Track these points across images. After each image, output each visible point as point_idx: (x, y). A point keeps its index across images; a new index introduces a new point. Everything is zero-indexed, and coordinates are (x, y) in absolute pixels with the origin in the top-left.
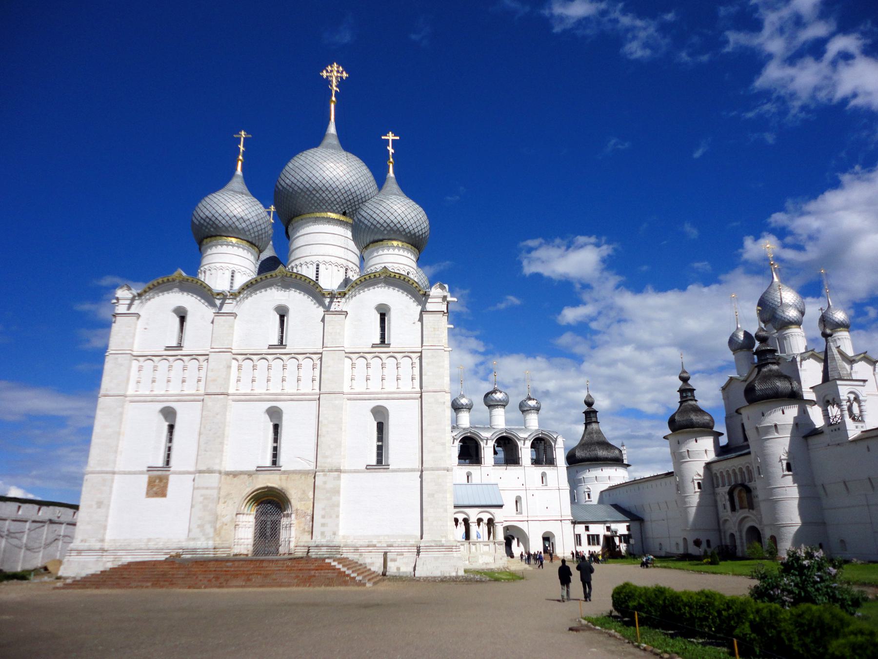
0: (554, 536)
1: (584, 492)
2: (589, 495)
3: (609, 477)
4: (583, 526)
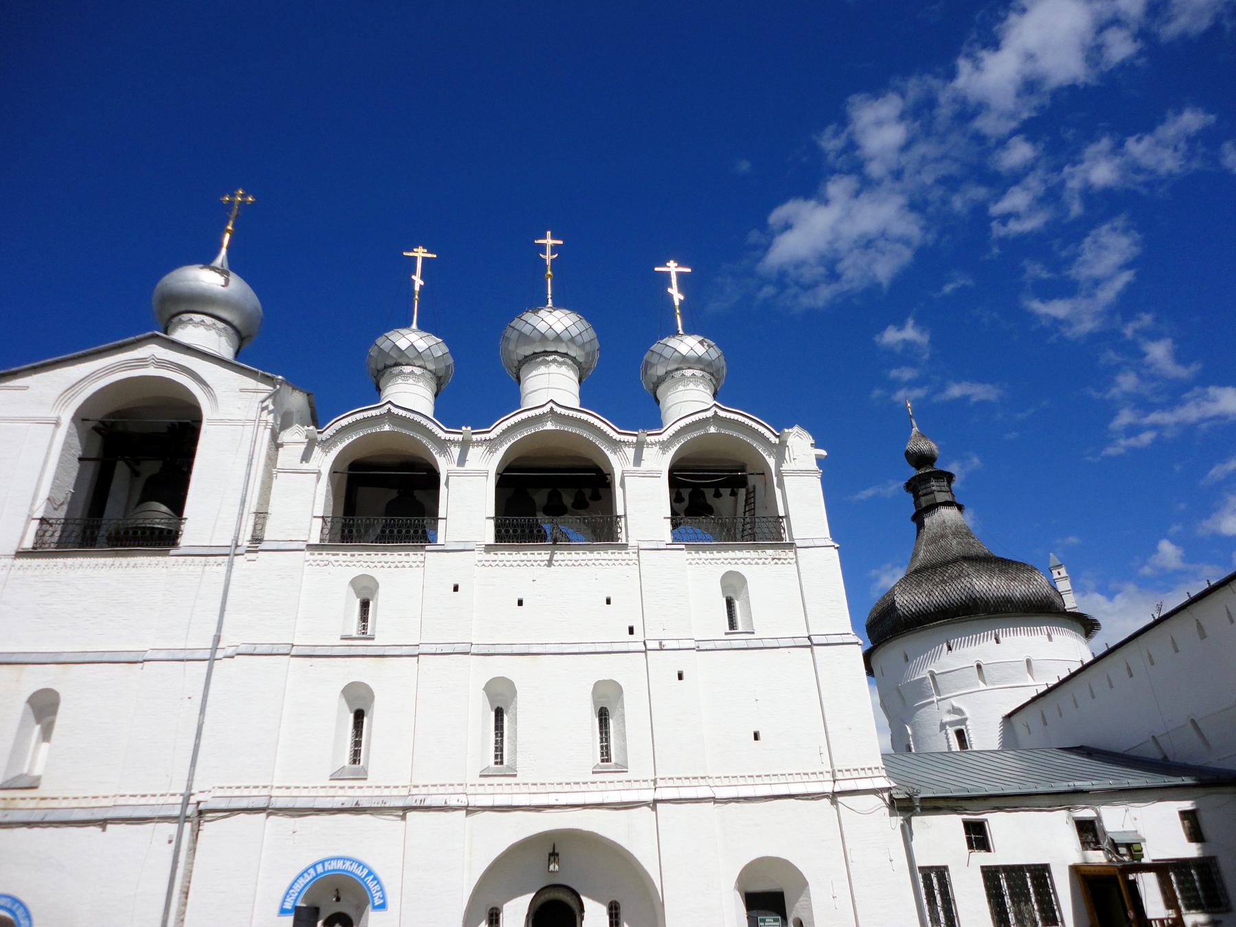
0: (802, 884)
1: (943, 726)
2: (960, 734)
3: (1028, 662)
4: (951, 826)
